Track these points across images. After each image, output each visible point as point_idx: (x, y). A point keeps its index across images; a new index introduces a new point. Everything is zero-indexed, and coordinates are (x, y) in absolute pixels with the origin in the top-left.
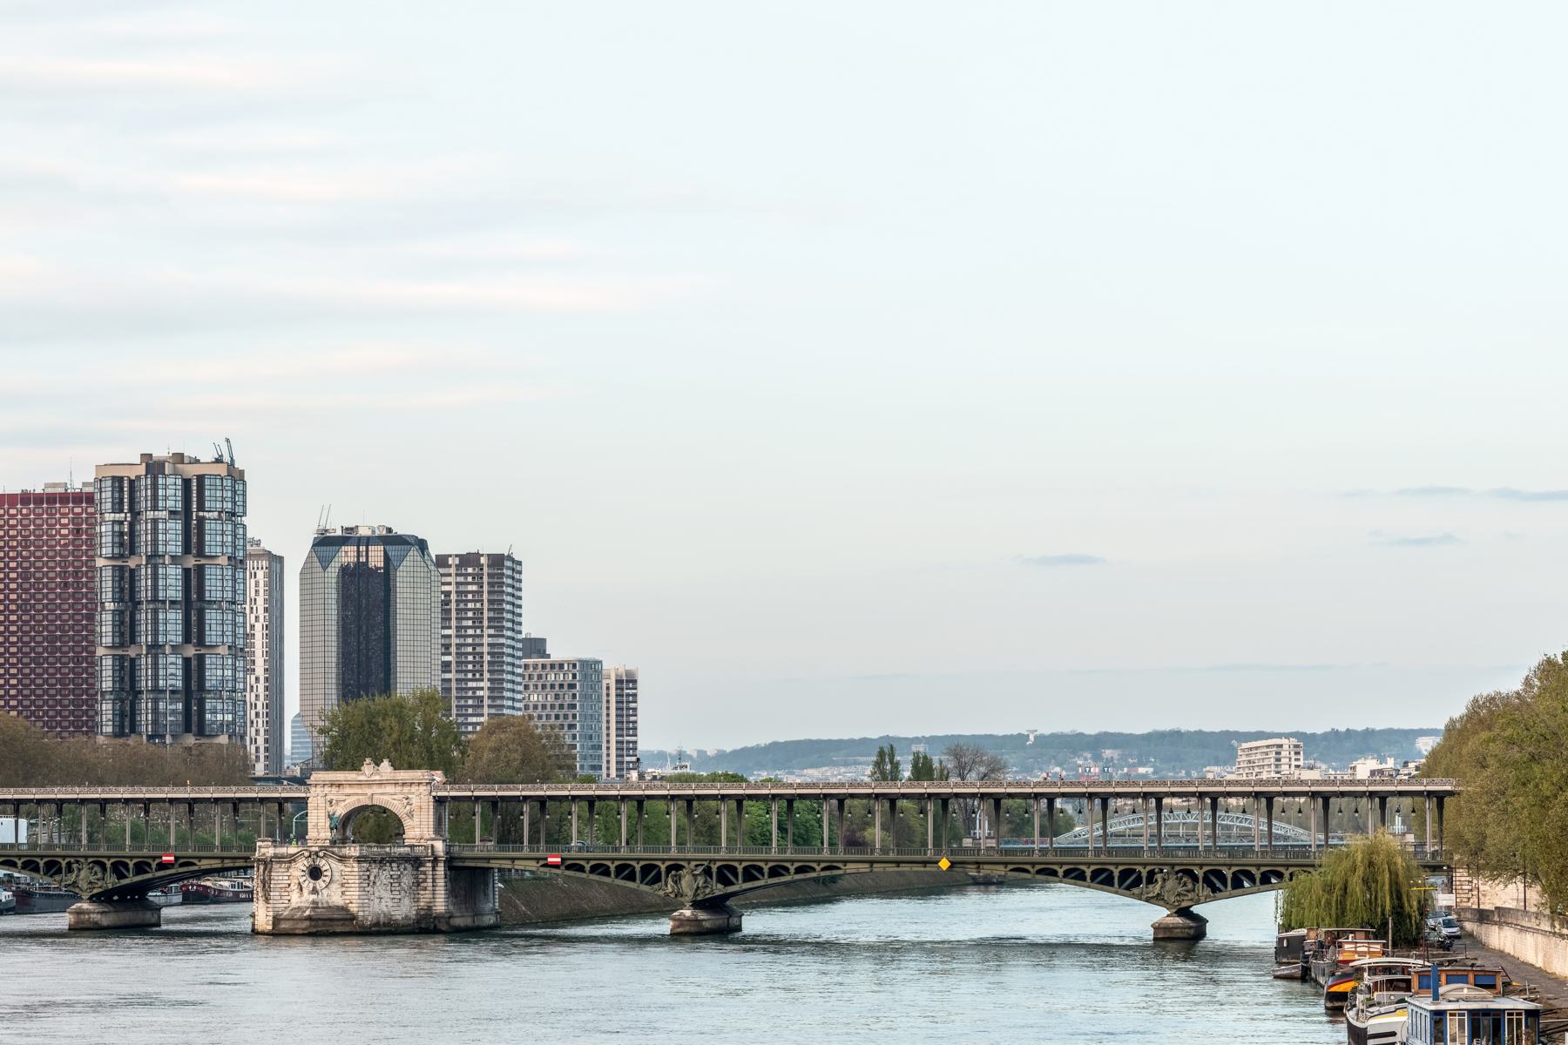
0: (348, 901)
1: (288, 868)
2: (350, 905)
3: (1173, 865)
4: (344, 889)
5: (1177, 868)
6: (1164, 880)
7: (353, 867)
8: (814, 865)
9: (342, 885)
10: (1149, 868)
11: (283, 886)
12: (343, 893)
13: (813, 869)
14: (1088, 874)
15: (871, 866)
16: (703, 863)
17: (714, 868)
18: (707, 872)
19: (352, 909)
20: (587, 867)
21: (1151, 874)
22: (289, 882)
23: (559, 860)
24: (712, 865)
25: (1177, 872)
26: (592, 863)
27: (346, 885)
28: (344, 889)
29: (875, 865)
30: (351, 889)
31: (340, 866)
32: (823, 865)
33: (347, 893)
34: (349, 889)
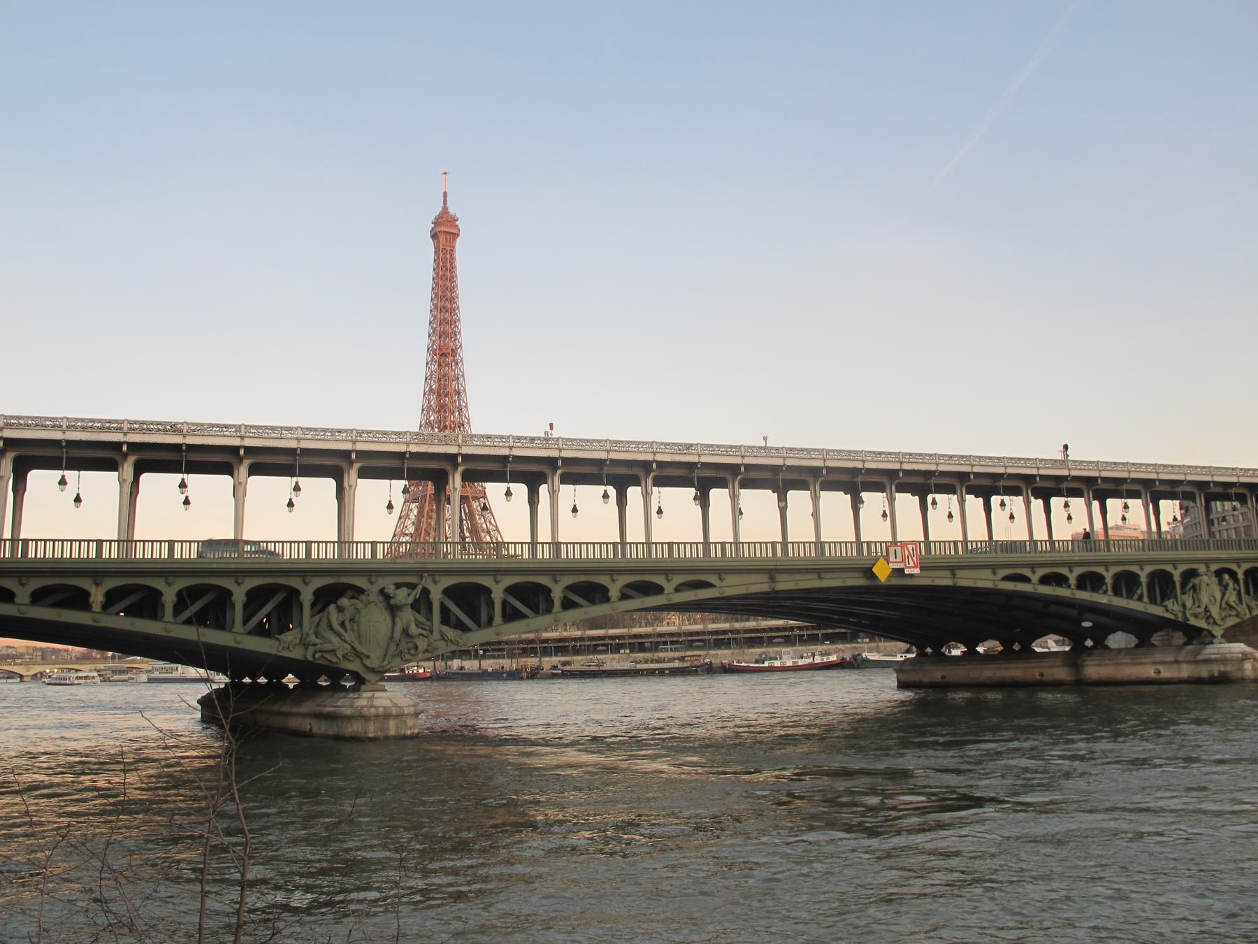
3: (1207, 562)
5: (1214, 567)
6: (1208, 585)
8: (659, 580)
10: (1182, 568)
13: (658, 590)
14: (1109, 580)
15: (772, 580)
16: (412, 580)
17: (436, 595)
18: (422, 603)
20: (97, 596)
21: (1190, 575)
24: (430, 586)
25: (1219, 573)
29: (779, 577)
32: (679, 579)
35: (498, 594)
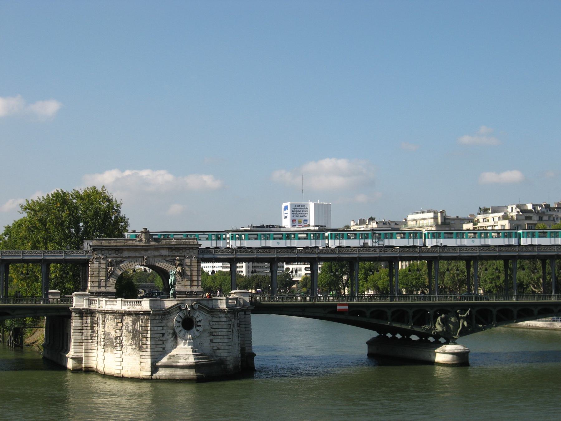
0: (215, 348)
1: (162, 319)
2: (218, 351)
4: (212, 337)
7: (220, 317)
9: (211, 334)
11: (158, 335)
12: (211, 341)
19: (219, 355)
22: (163, 332)
23: (347, 307)
26: (372, 310)
27: (214, 333)
28: (212, 337)
30: (219, 337)
31: (209, 317)
33: (215, 341)
34: (216, 337)
35: (495, 312)
